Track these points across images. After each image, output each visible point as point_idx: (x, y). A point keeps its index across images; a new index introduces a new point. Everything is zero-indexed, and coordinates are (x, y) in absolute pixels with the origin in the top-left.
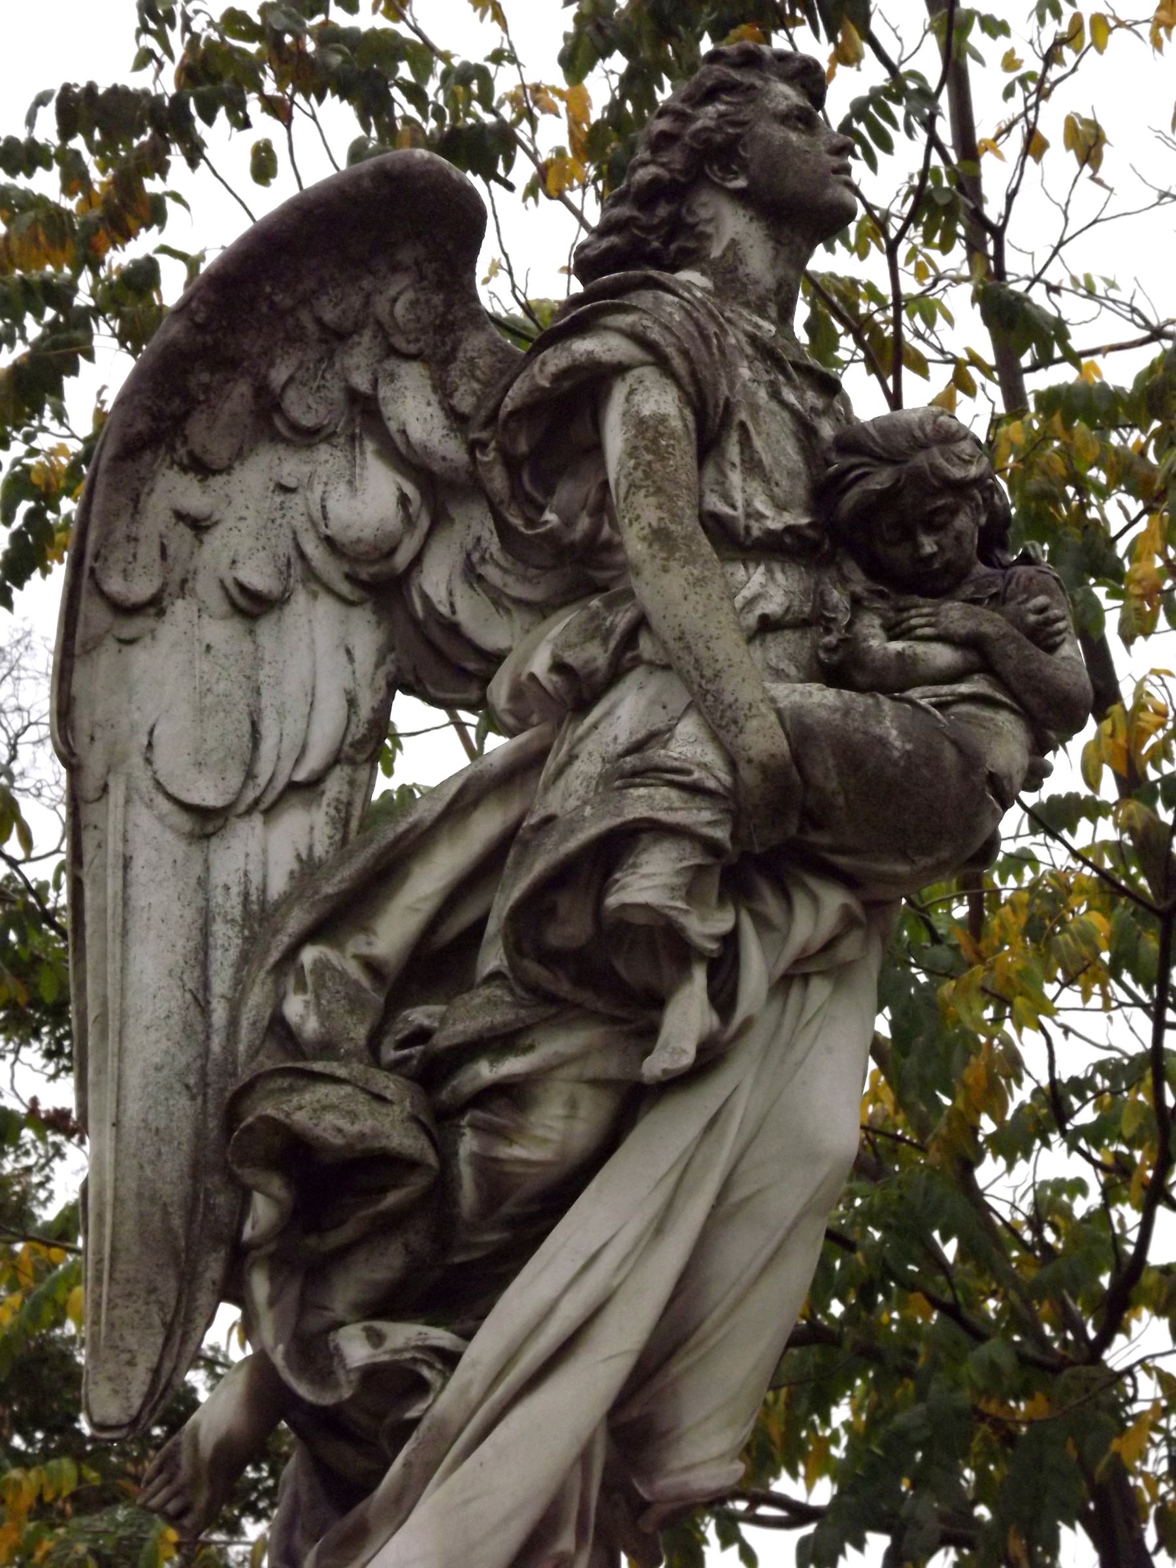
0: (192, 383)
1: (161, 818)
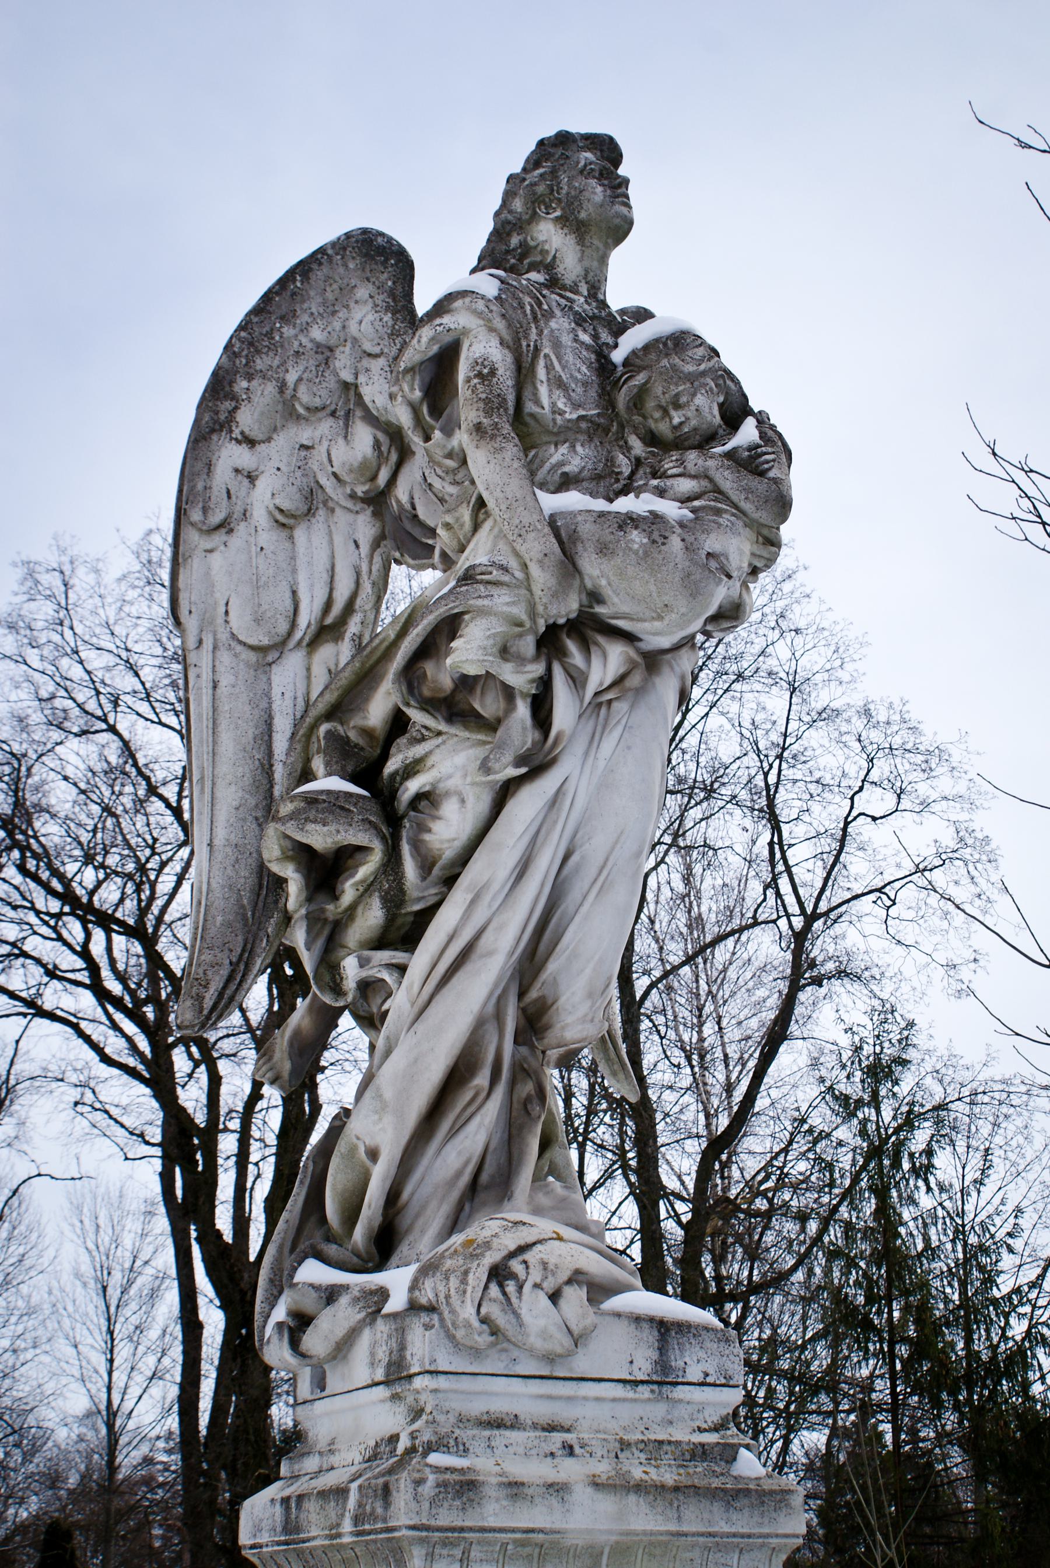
0: (236, 388)
1: (236, 655)
